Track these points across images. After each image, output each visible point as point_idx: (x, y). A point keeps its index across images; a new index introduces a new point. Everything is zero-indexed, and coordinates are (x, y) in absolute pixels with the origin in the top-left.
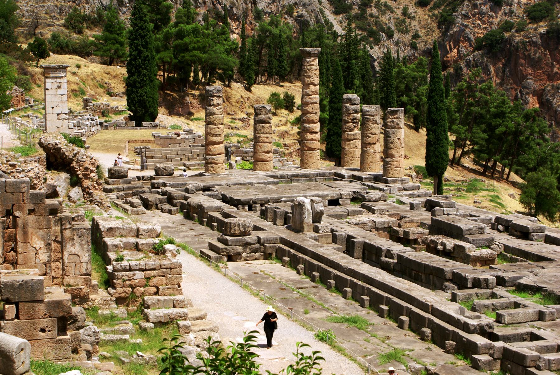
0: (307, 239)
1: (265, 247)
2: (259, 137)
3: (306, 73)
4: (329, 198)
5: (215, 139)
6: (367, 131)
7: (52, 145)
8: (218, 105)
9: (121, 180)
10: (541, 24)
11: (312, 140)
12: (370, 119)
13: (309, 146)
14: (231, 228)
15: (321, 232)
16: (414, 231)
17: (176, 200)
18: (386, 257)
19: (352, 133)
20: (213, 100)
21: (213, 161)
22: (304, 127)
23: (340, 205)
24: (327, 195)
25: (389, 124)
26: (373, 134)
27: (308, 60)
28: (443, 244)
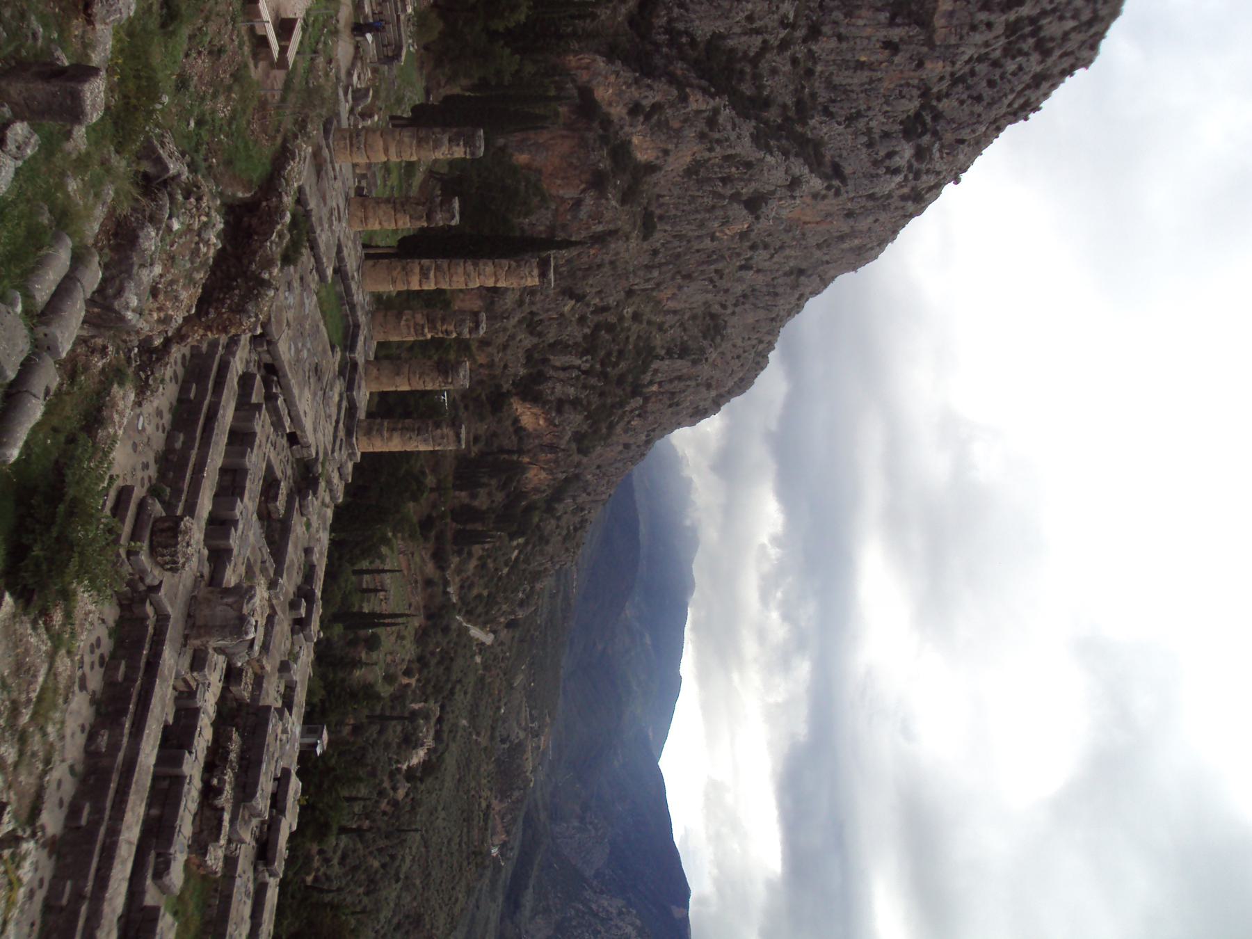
0: (172, 661)
1: (143, 602)
4: (298, 433)
5: (393, 150)
7: (277, 207)
10: (608, 162)
11: (409, 283)
12: (447, 377)
14: (166, 547)
15: (195, 674)
16: (244, 691)
18: (158, 855)
19: (426, 330)
20: (458, 145)
22: (429, 269)
23: (291, 446)
24: (303, 431)
25: (439, 431)
28: (219, 791)
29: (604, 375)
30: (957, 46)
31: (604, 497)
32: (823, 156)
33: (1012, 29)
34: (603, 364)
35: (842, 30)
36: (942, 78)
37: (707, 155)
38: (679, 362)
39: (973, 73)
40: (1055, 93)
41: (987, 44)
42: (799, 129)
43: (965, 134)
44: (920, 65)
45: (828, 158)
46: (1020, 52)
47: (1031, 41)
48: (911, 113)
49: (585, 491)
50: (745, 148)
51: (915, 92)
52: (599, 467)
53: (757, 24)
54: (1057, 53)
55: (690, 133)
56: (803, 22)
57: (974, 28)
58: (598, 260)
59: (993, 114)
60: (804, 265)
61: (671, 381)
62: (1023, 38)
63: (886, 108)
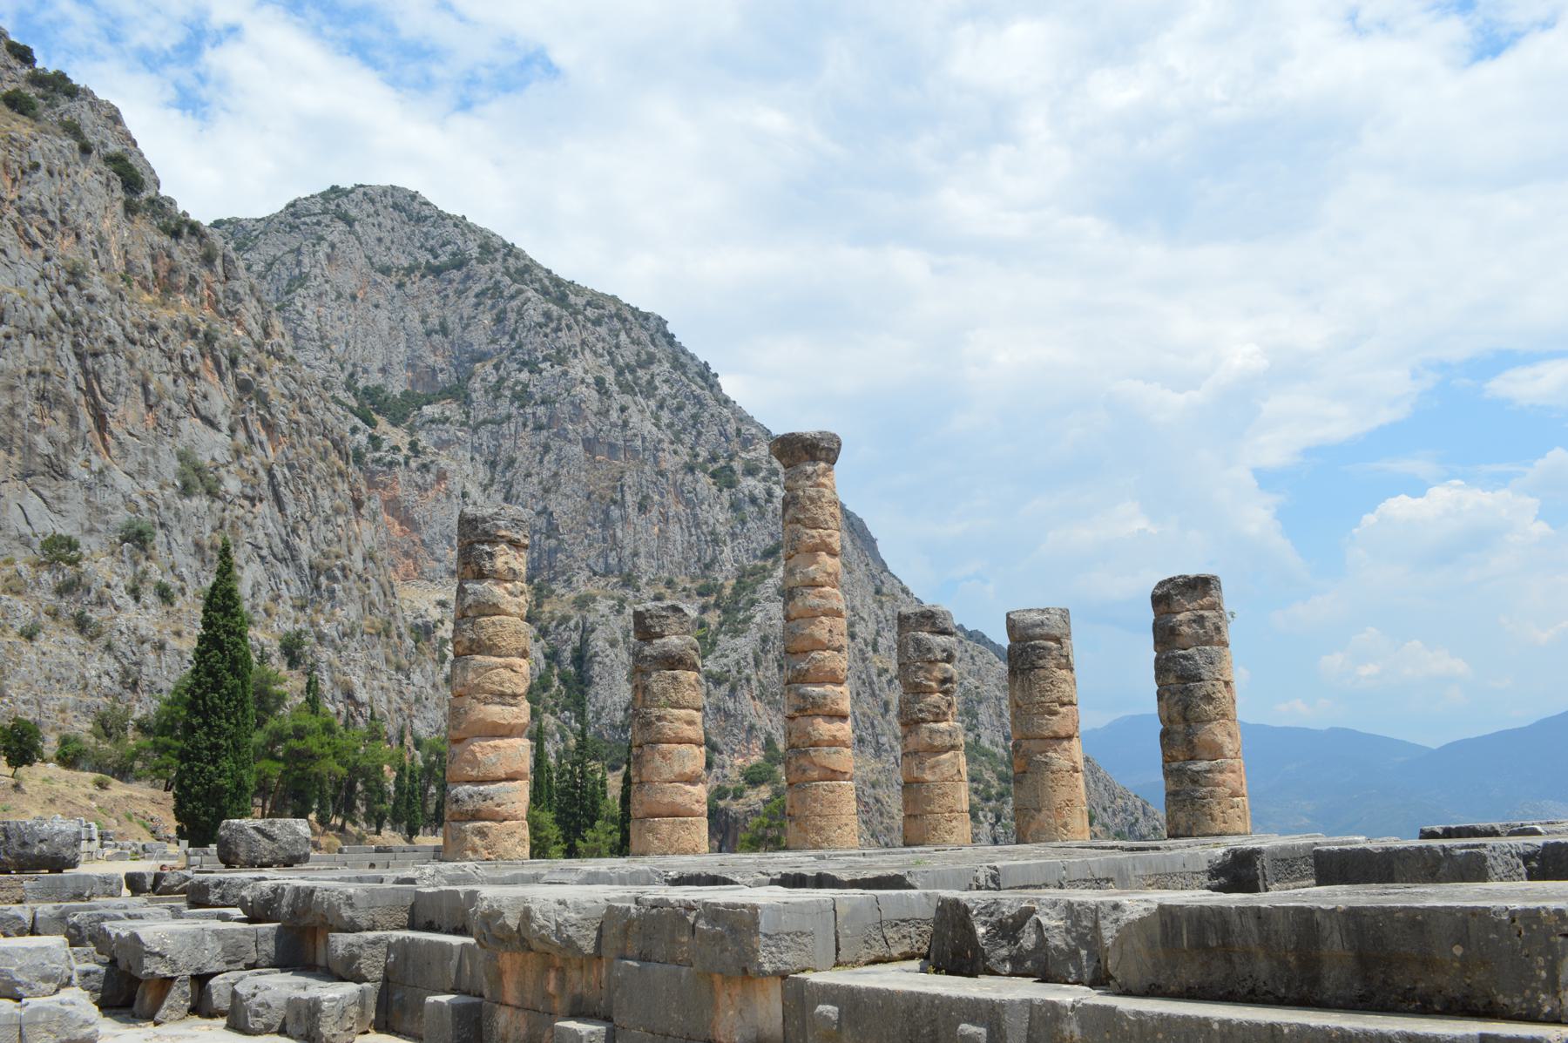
2: (659, 718)
3: (804, 509)
5: (496, 713)
6: (1042, 691)
8: (515, 574)
9: (28, 882)
11: (834, 742)
12: (1050, 649)
13: (825, 763)
17: (353, 927)
19: (943, 725)
20: (491, 555)
21: (482, 805)
22: (804, 697)
25: (1185, 629)
26: (1063, 704)
27: (809, 469)
29: (1001, 796)
30: (644, 439)
31: (1139, 804)
32: (755, 566)
33: (626, 389)
34: (988, 799)
35: (627, 552)
36: (676, 452)
37: (754, 683)
38: (983, 718)
39: (670, 426)
40: (691, 351)
41: (642, 411)
42: (727, 592)
43: (731, 428)
44: (661, 473)
45: (760, 563)
46: (650, 382)
47: (640, 372)
48: (711, 481)
49: (1133, 825)
50: (746, 644)
51: (689, 478)
52: (1105, 810)
53: (619, 636)
54: (652, 349)
55: (730, 704)
56: (619, 592)
57: (625, 424)
58: (871, 801)
59: (711, 402)
60: (872, 589)
61: (1003, 726)
62: (636, 379)
63: (705, 507)
